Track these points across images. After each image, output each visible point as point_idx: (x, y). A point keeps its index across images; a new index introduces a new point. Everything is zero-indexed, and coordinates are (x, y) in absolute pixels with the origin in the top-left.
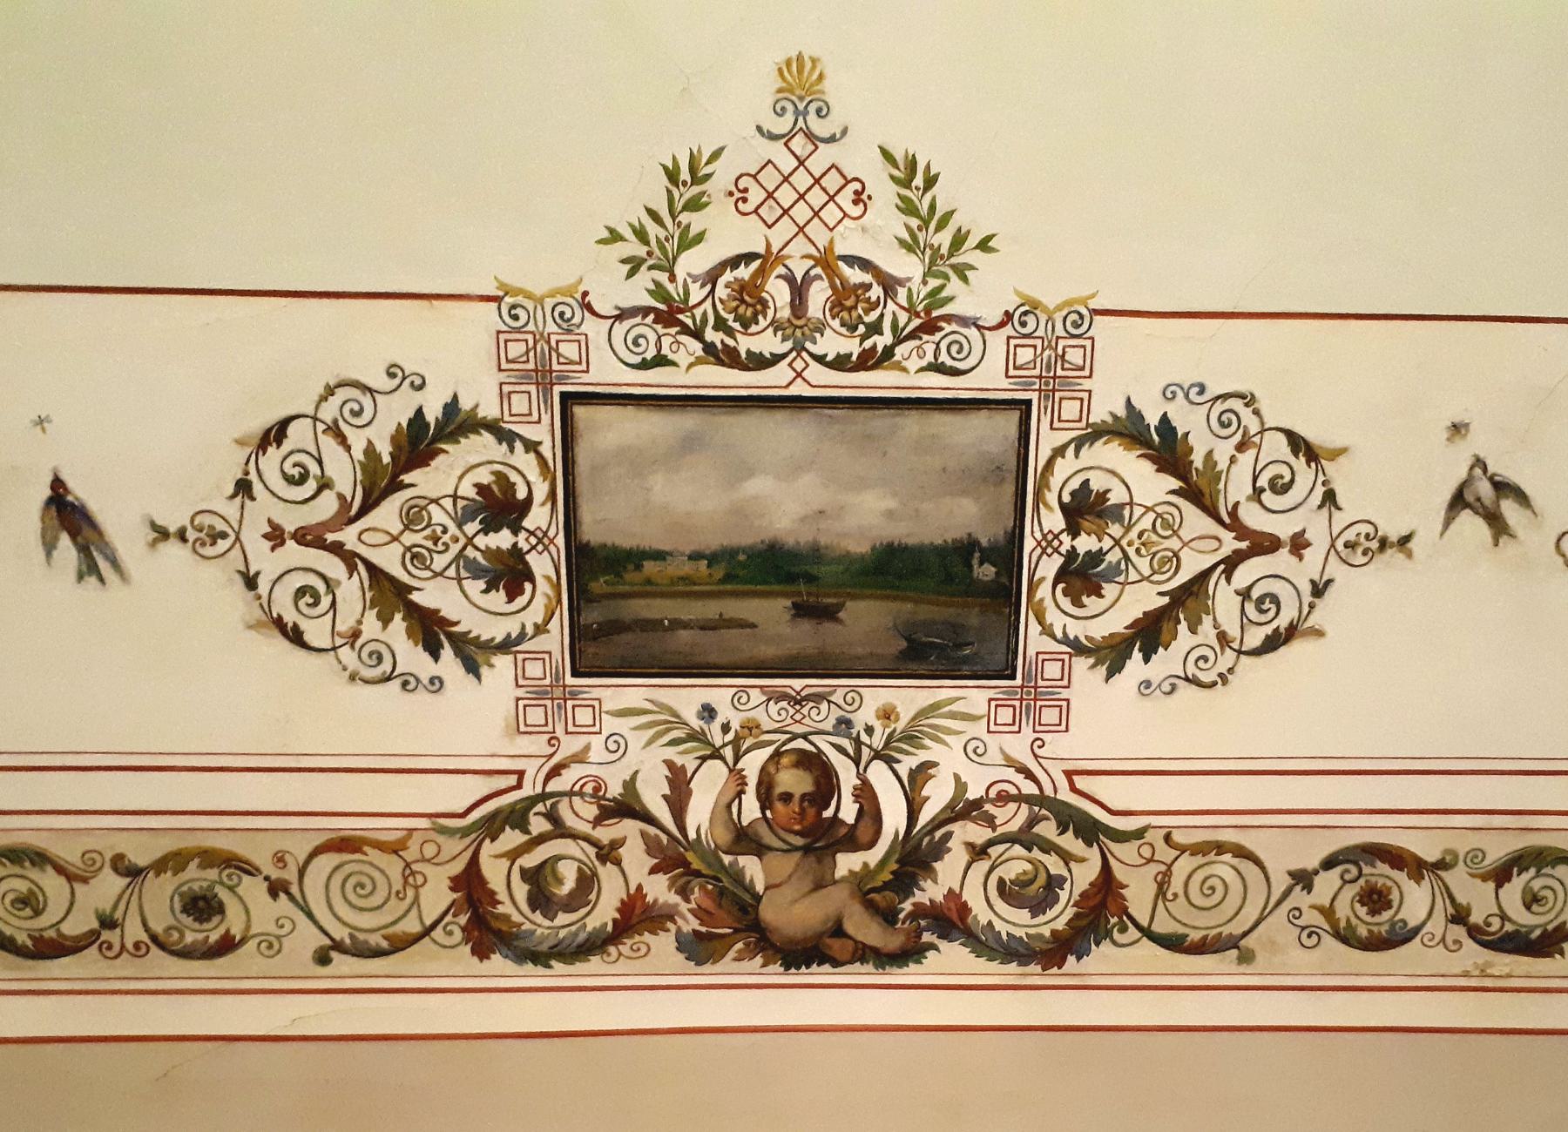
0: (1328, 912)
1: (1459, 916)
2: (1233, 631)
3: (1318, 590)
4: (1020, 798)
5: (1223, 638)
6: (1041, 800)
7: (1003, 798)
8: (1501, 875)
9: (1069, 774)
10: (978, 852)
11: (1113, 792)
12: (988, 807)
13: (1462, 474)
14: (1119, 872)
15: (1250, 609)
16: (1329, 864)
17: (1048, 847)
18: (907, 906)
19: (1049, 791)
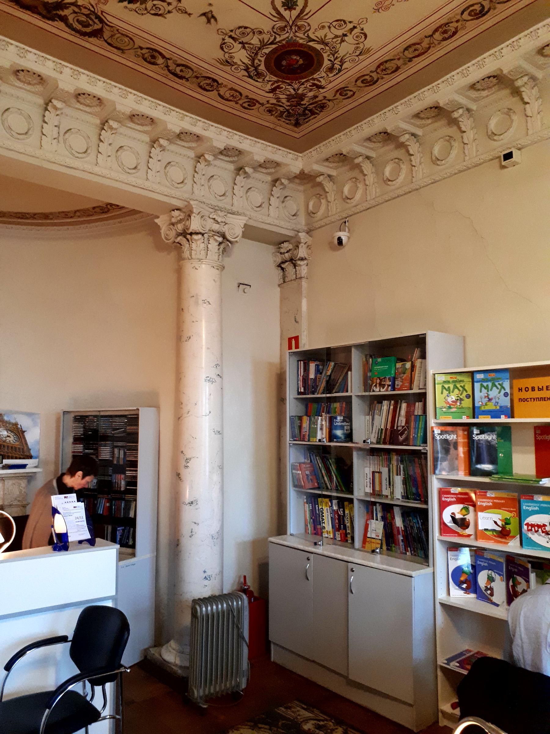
0: (143, 55)
1: (167, 66)
2: (149, 9)
3: (169, 12)
4: (89, 10)
5: (146, 9)
6: (94, 12)
7: (85, 8)
8: (178, 65)
9: (102, 12)
10: (74, 12)
11: (109, 18)
12: (82, 8)
13: (207, 11)
14: (104, 29)
15: (154, 8)
16: (148, 48)
17: (91, 19)
18: (55, 12)
19: (96, 12)
